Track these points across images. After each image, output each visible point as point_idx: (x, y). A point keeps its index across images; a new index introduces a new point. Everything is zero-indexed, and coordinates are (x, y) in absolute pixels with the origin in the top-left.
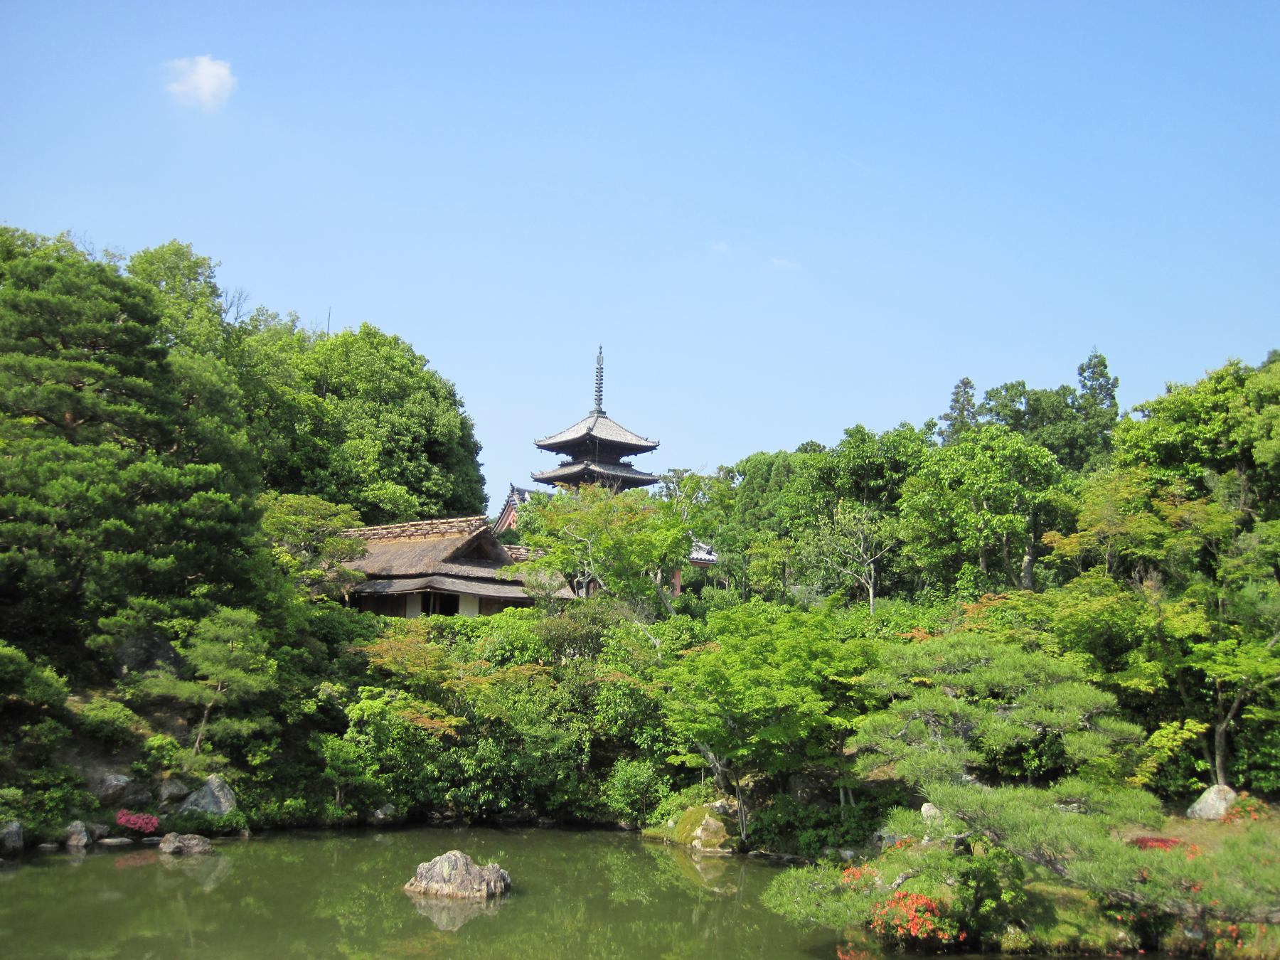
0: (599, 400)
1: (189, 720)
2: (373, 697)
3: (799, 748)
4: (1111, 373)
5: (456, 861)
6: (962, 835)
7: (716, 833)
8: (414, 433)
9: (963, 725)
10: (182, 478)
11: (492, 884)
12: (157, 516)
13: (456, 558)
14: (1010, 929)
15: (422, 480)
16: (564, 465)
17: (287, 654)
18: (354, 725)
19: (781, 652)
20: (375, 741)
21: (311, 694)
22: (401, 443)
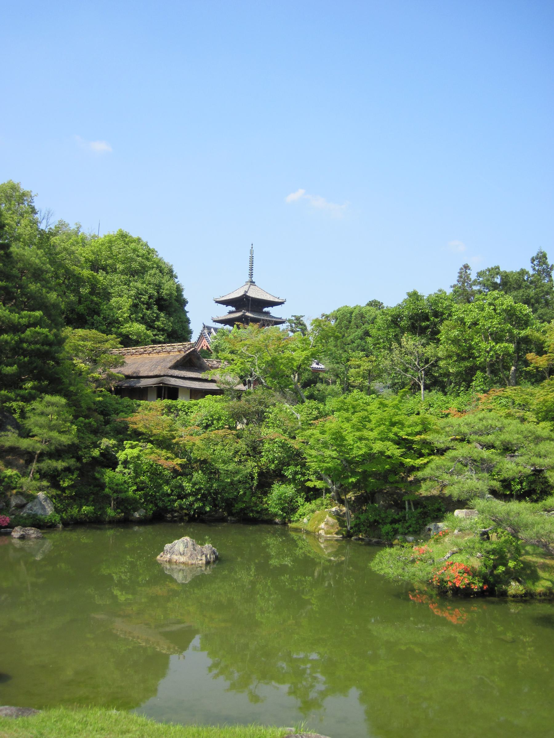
0: (251, 275)
1: (26, 461)
2: (132, 447)
3: (384, 477)
5: (187, 543)
6: (486, 530)
7: (333, 526)
8: (150, 293)
9: (488, 465)
10: (20, 320)
11: (208, 556)
12: (6, 342)
13: (176, 366)
14: (513, 583)
15: (154, 321)
16: (230, 312)
17: (82, 422)
18: (122, 464)
19: (374, 422)
20: (134, 473)
21: (96, 446)
22: (142, 299)
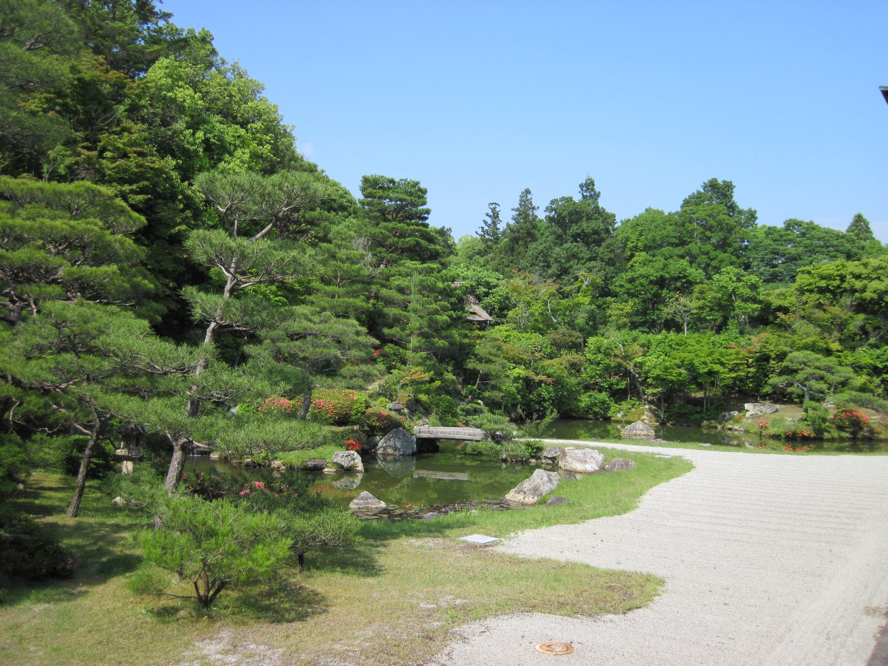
4: (597, 188)
7: (651, 417)
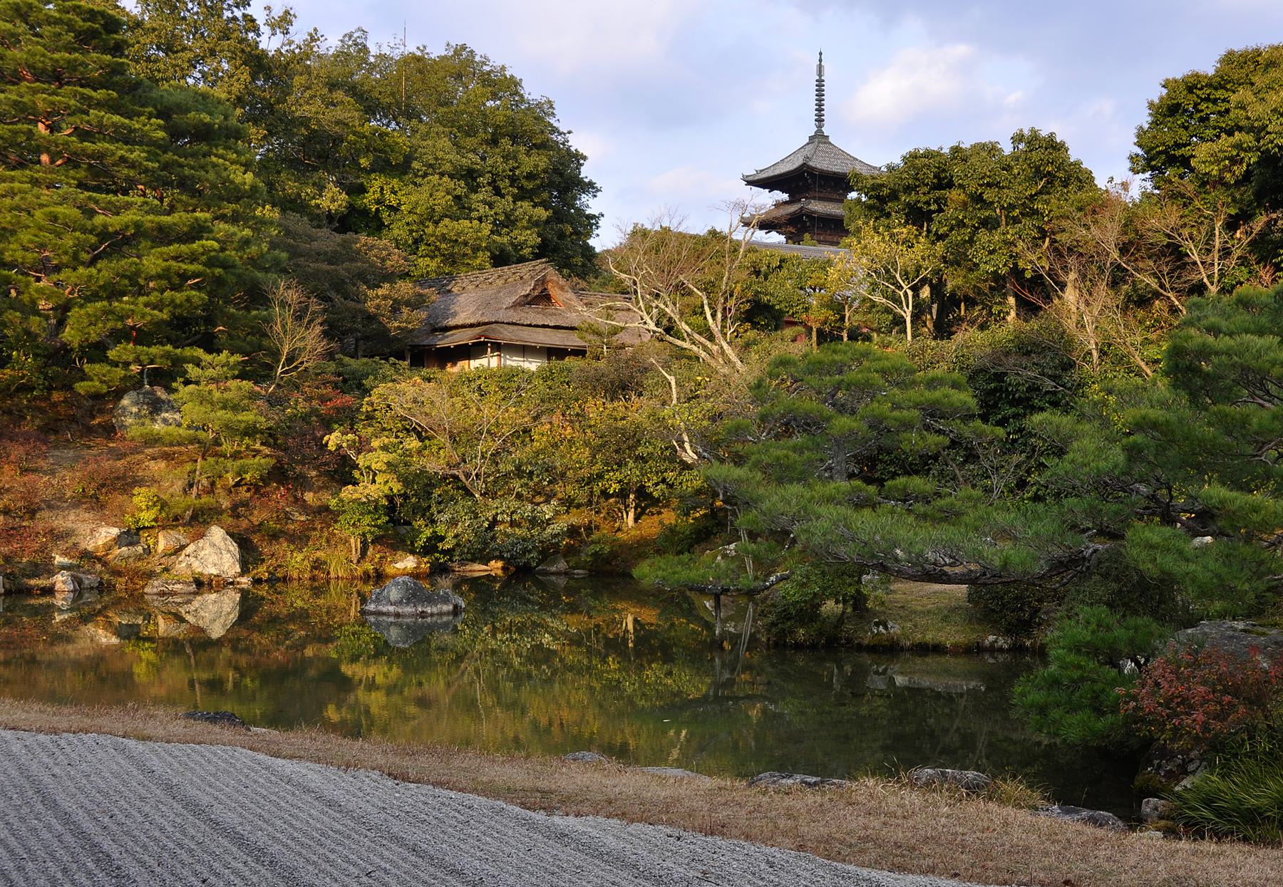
0: (820, 120)
16: (778, 205)
